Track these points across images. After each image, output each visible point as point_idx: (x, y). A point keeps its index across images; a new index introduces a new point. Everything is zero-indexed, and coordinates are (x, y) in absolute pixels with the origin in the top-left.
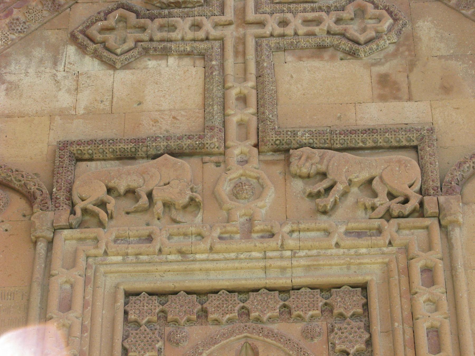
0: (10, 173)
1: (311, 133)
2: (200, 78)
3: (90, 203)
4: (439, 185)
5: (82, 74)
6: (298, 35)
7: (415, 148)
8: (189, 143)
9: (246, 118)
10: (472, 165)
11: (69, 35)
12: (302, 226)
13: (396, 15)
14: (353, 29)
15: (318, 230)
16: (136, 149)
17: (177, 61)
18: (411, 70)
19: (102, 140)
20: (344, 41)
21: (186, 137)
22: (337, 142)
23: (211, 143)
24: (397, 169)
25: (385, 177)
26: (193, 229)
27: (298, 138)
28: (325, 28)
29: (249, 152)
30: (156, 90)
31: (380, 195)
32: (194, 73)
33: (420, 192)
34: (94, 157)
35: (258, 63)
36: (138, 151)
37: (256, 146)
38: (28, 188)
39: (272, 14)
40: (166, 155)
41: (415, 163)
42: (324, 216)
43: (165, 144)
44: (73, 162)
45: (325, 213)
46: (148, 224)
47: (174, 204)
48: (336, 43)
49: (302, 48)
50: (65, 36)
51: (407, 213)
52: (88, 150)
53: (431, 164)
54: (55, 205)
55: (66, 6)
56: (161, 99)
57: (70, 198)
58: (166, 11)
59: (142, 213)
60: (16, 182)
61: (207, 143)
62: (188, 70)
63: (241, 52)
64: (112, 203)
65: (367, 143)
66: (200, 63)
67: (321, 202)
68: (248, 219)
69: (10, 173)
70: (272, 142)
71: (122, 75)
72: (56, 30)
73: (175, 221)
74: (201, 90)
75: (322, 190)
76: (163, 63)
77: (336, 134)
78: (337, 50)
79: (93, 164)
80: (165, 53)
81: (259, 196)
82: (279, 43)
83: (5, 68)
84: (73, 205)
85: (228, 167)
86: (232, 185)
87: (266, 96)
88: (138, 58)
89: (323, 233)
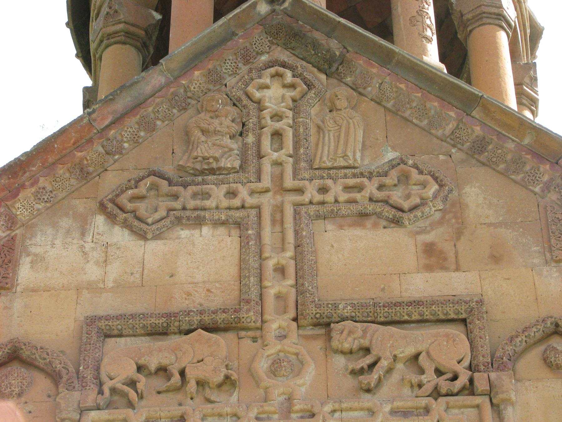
0: (34, 351)
1: (353, 305)
2: (235, 248)
3: (119, 382)
4: (489, 360)
5: (111, 245)
6: (339, 203)
7: (464, 321)
8: (224, 317)
9: (284, 290)
10: (524, 339)
11: (98, 204)
12: (344, 405)
13: (441, 181)
14: (396, 196)
15: (362, 409)
16: (168, 324)
17: (211, 231)
18: (458, 239)
19: (132, 315)
20: (387, 208)
21: (221, 311)
22: (382, 315)
23: (247, 318)
24: (445, 343)
25: (432, 353)
26: (229, 410)
27: (339, 312)
28: (367, 195)
29: (288, 326)
30: (189, 262)
31: (427, 371)
32: (229, 243)
33: (470, 368)
34: (124, 333)
35: (296, 232)
36: (170, 326)
37: (295, 319)
38: (54, 366)
39: (311, 180)
40: (200, 330)
41: (464, 337)
42: (367, 394)
43: (199, 318)
44: (102, 339)
45: (368, 391)
46: (180, 405)
47: (208, 383)
49: (343, 216)
50: (94, 205)
51: (456, 391)
52: (116, 325)
53: (480, 338)
54: (82, 385)
55: (95, 174)
56: (195, 270)
57: (97, 377)
58: (200, 179)
59: (174, 393)
60: (40, 360)
61: (243, 318)
62: (223, 240)
63: (278, 220)
64: (142, 382)
65: (413, 315)
66: (235, 233)
67: (364, 379)
68: (287, 398)
69: (34, 351)
70: (312, 316)
71: (152, 245)
72: (85, 199)
73: (209, 401)
74: (236, 261)
75: (366, 367)
76: (196, 232)
77: (380, 307)
79: (123, 340)
80: (199, 222)
81: (298, 374)
82: (318, 211)
83: (30, 239)
84: (101, 384)
85: (265, 343)
86: (270, 362)
87: (306, 267)
88: (170, 228)
89: (366, 413)
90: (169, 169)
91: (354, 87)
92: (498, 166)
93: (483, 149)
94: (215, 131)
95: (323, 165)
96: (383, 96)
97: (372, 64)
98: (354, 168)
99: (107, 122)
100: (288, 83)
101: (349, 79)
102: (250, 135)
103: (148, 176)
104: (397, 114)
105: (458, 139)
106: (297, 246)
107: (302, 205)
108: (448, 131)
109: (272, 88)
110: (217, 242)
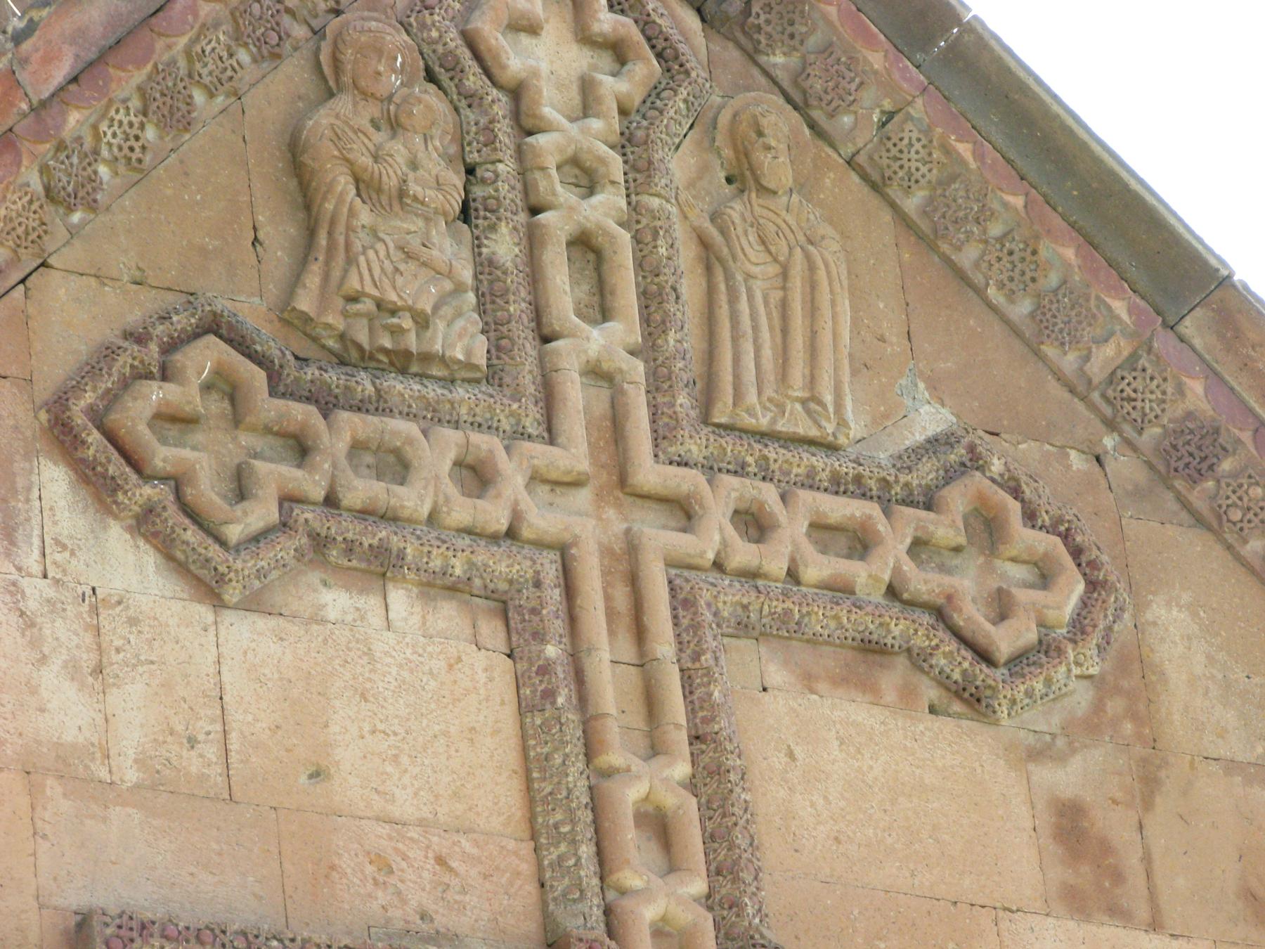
2: (503, 703)
6: (798, 582)
11: (43, 416)
18: (1148, 805)
28: (886, 577)
32: (482, 677)
48: (920, 641)
56: (389, 769)
58: (365, 384)
66: (492, 631)
71: (242, 631)
74: (512, 758)
76: (371, 603)
78: (922, 670)
80: (380, 568)
82: (745, 607)
90: (251, 310)
91: (797, 97)
92: (1246, 542)
93: (1204, 466)
94: (402, 194)
95: (748, 421)
96: (896, 166)
97: (867, 29)
98: (832, 448)
99: (60, 73)
100: (601, 34)
101: (779, 59)
102: (504, 229)
103: (197, 335)
104: (933, 247)
105: (1128, 407)
106: (696, 738)
107: (690, 567)
108: (1097, 368)
109: (544, 33)
110: (443, 664)
